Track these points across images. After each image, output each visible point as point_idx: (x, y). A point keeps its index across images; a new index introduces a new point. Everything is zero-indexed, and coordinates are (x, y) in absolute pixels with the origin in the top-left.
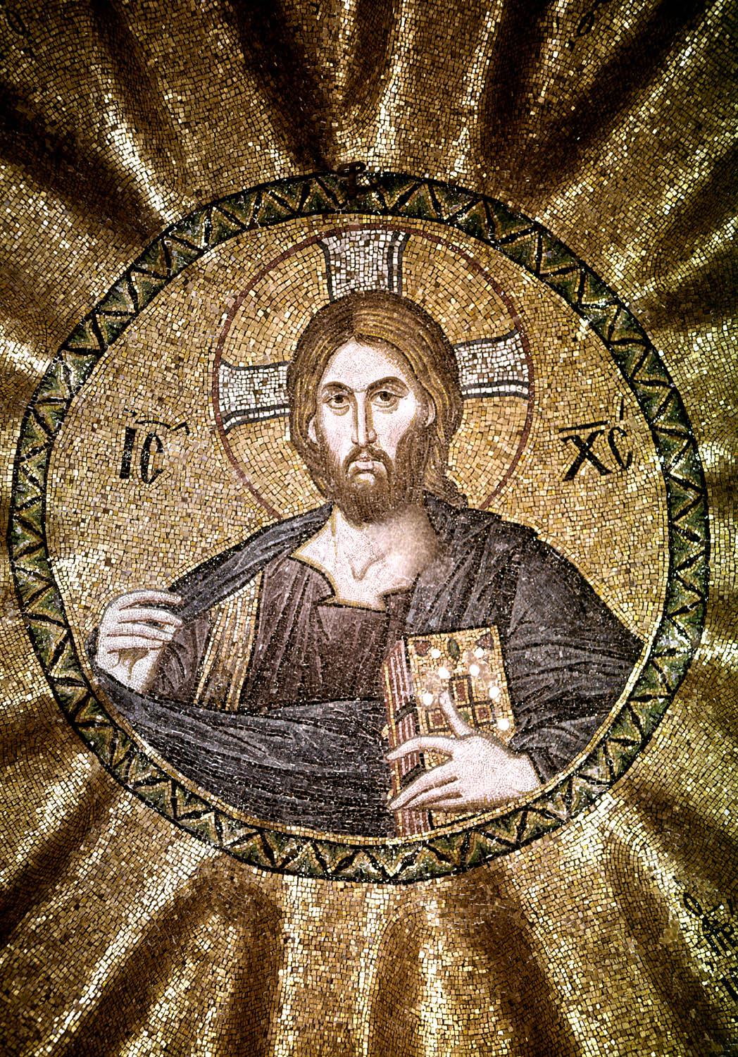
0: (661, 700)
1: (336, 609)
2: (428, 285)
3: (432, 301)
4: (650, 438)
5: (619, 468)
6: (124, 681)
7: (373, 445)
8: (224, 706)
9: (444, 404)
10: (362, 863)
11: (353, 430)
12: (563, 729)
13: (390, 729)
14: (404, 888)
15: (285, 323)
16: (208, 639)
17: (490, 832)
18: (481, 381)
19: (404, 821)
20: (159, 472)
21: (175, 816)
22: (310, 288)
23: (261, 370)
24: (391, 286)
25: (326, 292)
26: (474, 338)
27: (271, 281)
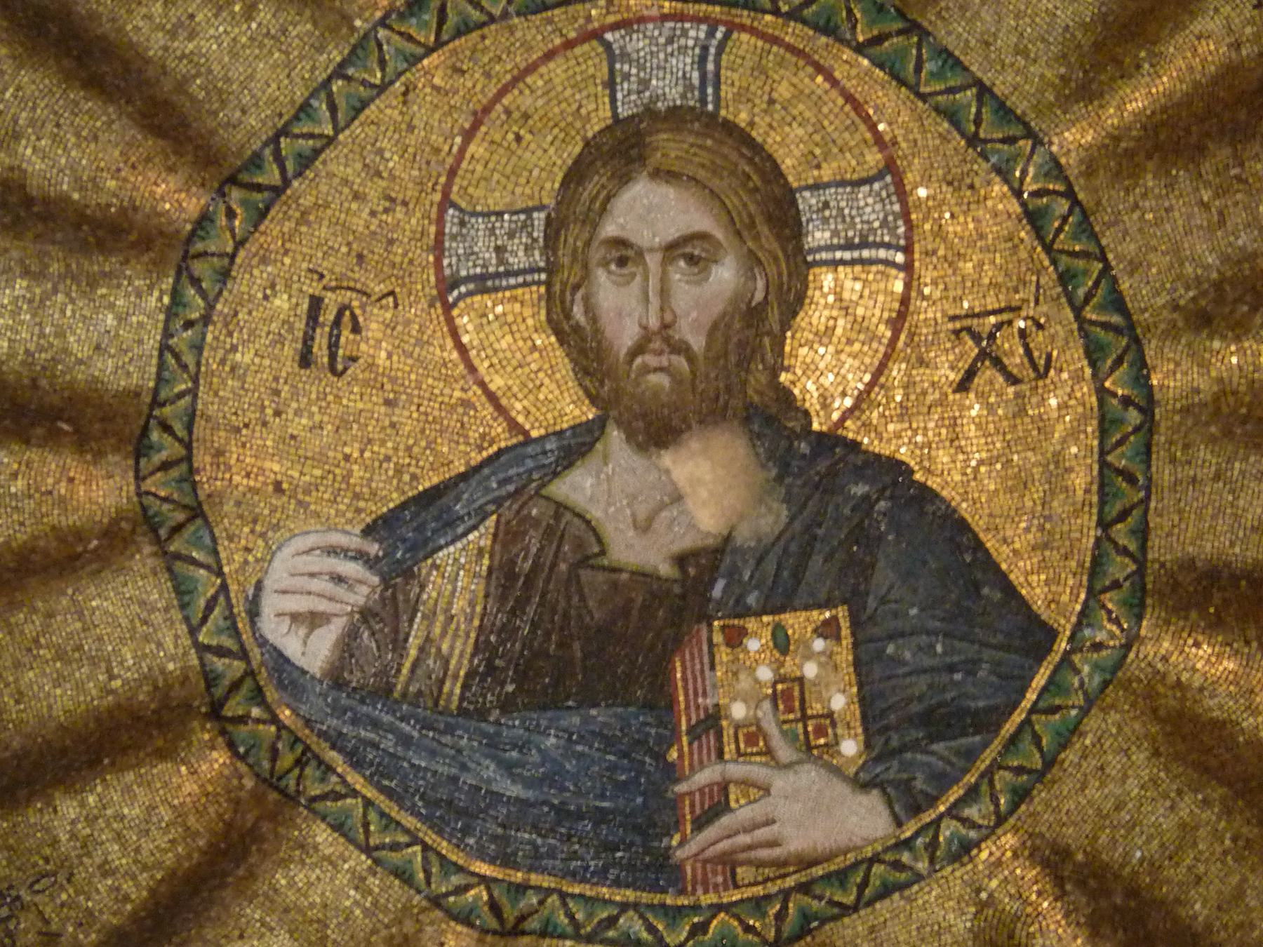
2: (757, 101)
5: (1032, 375)
7: (671, 332)
8: (436, 704)
9: (780, 275)
11: (640, 309)
12: (933, 753)
13: (680, 750)
16: (415, 611)
17: (818, 892)
18: (835, 241)
20: (354, 359)
24: (703, 101)
25: (608, 107)
26: (826, 179)
27: (527, 92)
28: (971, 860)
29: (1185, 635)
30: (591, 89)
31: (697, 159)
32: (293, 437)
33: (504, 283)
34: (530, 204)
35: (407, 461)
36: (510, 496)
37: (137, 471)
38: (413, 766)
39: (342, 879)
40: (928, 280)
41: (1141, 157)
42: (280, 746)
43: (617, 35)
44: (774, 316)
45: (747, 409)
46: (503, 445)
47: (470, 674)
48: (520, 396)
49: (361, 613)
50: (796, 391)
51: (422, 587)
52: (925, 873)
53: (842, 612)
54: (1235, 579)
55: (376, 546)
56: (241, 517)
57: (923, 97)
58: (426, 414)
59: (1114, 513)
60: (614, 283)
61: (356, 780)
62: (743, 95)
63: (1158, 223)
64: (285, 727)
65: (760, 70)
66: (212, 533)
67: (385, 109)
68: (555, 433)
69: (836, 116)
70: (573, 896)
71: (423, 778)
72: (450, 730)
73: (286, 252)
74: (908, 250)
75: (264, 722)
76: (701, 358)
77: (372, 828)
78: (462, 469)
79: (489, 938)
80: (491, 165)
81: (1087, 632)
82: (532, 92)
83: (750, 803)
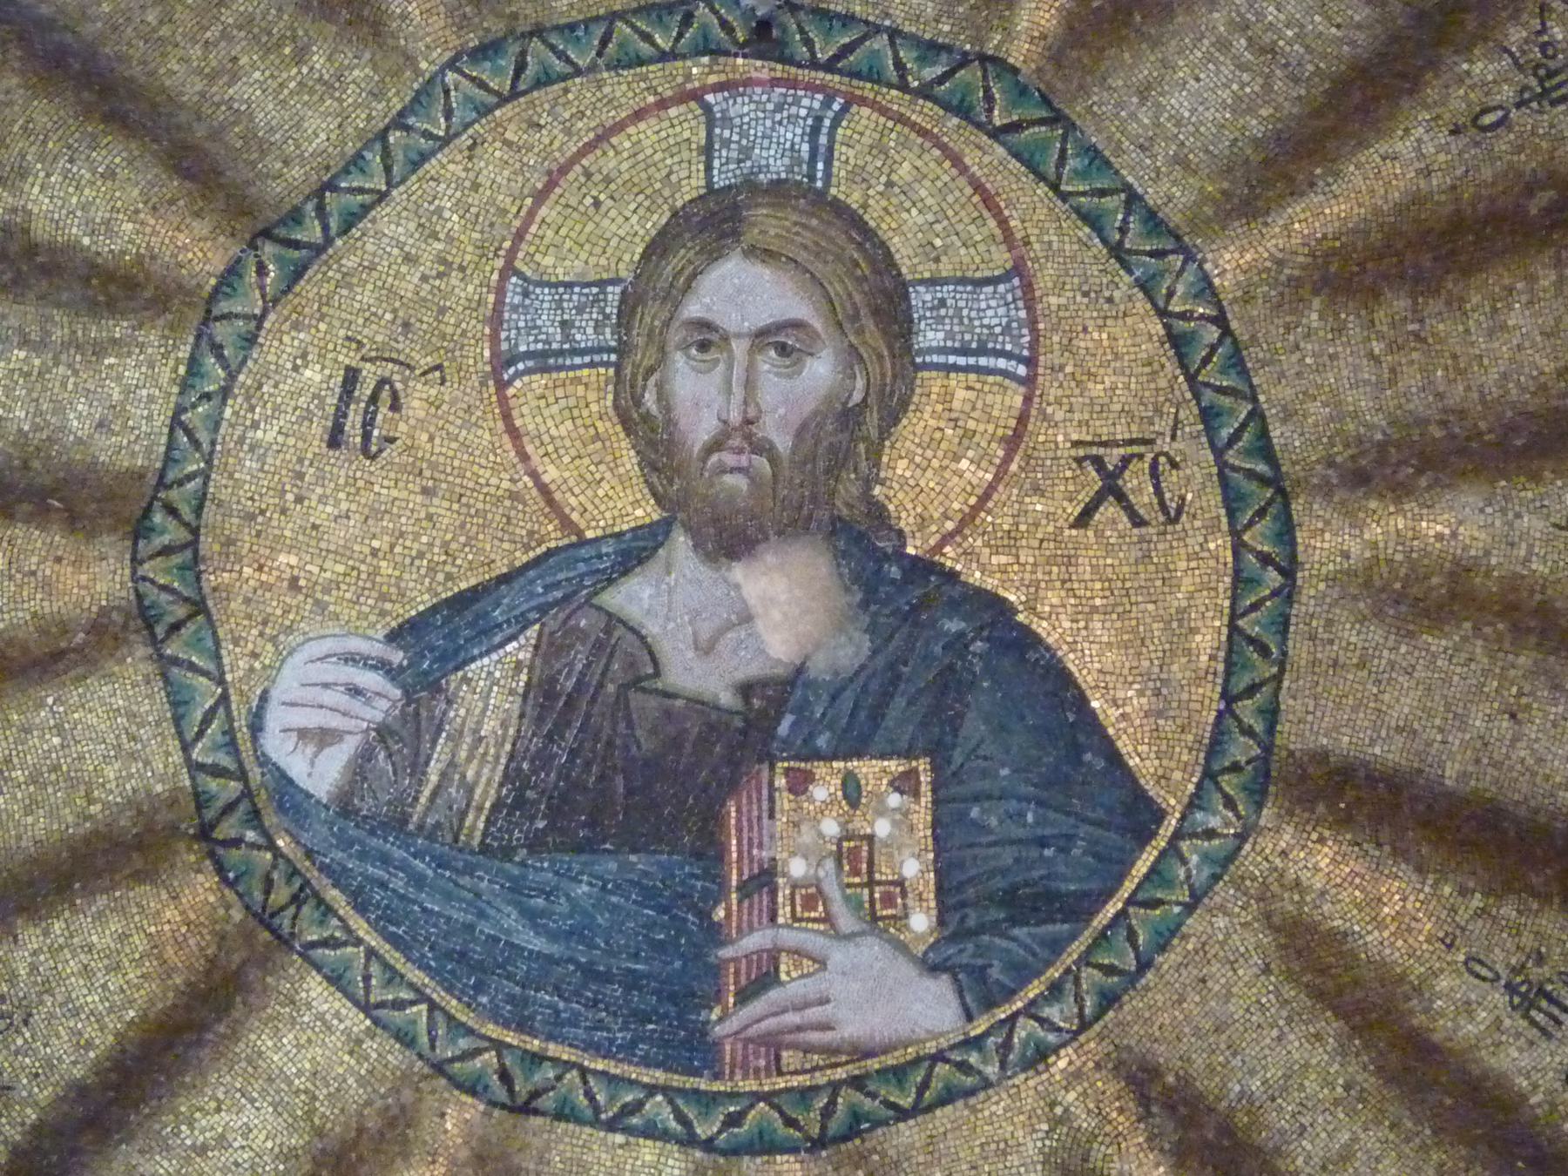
0: (1177, 909)
1: (659, 699)
3: (878, 208)
4: (1215, 478)
5: (1162, 518)
6: (304, 782)
8: (456, 840)
9: (883, 375)
10: (659, 1109)
11: (721, 399)
12: (1014, 939)
14: (722, 1160)
15: (627, 219)
16: (440, 729)
18: (949, 344)
19: (733, 1058)
20: (392, 440)
21: (367, 1001)
22: (676, 168)
23: (577, 289)
24: (812, 178)
25: (702, 175)
26: (944, 274)
27: (611, 153)
28: (1048, 1067)
29: (1309, 828)
30: (685, 155)
31: (799, 239)
32: (315, 527)
33: (568, 362)
34: (605, 276)
35: (443, 558)
36: (557, 603)
37: (135, 552)
38: (424, 910)
39: (334, 1041)
40: (1051, 399)
41: (1305, 292)
42: (275, 876)
43: (720, 96)
44: (872, 419)
45: (833, 524)
46: (553, 544)
47: (496, 807)
48: (577, 490)
49: (377, 730)
50: (891, 507)
51: (449, 702)
52: (993, 1078)
53: (922, 765)
54: (1372, 779)
55: (401, 654)
56: (249, 617)
57: (1064, 197)
58: (468, 506)
59: (1242, 686)
60: (693, 369)
61: (360, 927)
62: (858, 175)
63: (1319, 369)
64: (282, 856)
65: (879, 148)
66: (215, 633)
67: (449, 164)
68: (611, 536)
69: (963, 207)
70: (595, 1072)
71: (435, 926)
72: (469, 870)
73: (321, 319)
74: (1031, 362)
75: (259, 848)
76: (786, 464)
77: (374, 982)
78: (505, 570)
79: (496, 1113)
80: (563, 232)
81: (1199, 816)
82: (617, 153)
83: (802, 976)
